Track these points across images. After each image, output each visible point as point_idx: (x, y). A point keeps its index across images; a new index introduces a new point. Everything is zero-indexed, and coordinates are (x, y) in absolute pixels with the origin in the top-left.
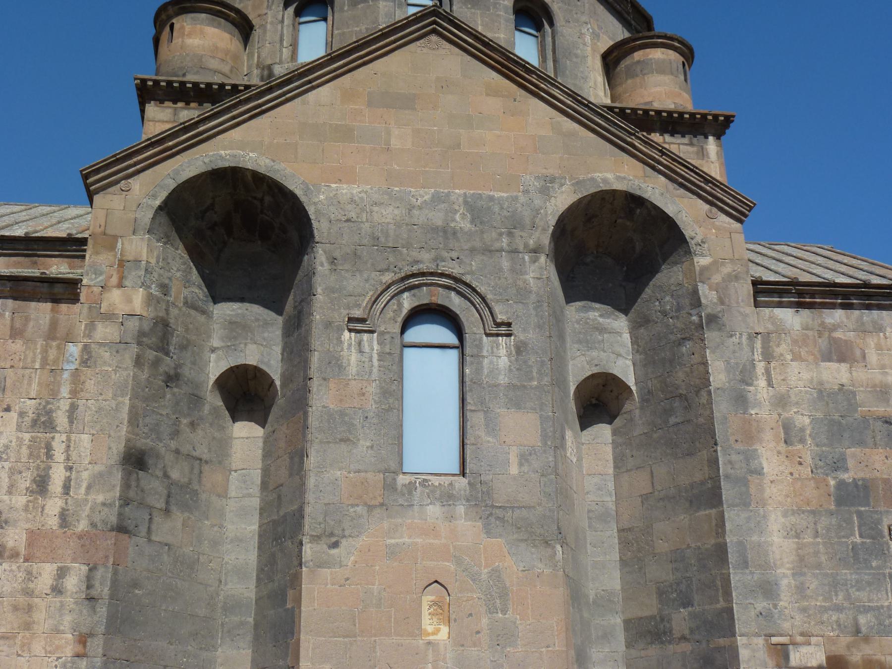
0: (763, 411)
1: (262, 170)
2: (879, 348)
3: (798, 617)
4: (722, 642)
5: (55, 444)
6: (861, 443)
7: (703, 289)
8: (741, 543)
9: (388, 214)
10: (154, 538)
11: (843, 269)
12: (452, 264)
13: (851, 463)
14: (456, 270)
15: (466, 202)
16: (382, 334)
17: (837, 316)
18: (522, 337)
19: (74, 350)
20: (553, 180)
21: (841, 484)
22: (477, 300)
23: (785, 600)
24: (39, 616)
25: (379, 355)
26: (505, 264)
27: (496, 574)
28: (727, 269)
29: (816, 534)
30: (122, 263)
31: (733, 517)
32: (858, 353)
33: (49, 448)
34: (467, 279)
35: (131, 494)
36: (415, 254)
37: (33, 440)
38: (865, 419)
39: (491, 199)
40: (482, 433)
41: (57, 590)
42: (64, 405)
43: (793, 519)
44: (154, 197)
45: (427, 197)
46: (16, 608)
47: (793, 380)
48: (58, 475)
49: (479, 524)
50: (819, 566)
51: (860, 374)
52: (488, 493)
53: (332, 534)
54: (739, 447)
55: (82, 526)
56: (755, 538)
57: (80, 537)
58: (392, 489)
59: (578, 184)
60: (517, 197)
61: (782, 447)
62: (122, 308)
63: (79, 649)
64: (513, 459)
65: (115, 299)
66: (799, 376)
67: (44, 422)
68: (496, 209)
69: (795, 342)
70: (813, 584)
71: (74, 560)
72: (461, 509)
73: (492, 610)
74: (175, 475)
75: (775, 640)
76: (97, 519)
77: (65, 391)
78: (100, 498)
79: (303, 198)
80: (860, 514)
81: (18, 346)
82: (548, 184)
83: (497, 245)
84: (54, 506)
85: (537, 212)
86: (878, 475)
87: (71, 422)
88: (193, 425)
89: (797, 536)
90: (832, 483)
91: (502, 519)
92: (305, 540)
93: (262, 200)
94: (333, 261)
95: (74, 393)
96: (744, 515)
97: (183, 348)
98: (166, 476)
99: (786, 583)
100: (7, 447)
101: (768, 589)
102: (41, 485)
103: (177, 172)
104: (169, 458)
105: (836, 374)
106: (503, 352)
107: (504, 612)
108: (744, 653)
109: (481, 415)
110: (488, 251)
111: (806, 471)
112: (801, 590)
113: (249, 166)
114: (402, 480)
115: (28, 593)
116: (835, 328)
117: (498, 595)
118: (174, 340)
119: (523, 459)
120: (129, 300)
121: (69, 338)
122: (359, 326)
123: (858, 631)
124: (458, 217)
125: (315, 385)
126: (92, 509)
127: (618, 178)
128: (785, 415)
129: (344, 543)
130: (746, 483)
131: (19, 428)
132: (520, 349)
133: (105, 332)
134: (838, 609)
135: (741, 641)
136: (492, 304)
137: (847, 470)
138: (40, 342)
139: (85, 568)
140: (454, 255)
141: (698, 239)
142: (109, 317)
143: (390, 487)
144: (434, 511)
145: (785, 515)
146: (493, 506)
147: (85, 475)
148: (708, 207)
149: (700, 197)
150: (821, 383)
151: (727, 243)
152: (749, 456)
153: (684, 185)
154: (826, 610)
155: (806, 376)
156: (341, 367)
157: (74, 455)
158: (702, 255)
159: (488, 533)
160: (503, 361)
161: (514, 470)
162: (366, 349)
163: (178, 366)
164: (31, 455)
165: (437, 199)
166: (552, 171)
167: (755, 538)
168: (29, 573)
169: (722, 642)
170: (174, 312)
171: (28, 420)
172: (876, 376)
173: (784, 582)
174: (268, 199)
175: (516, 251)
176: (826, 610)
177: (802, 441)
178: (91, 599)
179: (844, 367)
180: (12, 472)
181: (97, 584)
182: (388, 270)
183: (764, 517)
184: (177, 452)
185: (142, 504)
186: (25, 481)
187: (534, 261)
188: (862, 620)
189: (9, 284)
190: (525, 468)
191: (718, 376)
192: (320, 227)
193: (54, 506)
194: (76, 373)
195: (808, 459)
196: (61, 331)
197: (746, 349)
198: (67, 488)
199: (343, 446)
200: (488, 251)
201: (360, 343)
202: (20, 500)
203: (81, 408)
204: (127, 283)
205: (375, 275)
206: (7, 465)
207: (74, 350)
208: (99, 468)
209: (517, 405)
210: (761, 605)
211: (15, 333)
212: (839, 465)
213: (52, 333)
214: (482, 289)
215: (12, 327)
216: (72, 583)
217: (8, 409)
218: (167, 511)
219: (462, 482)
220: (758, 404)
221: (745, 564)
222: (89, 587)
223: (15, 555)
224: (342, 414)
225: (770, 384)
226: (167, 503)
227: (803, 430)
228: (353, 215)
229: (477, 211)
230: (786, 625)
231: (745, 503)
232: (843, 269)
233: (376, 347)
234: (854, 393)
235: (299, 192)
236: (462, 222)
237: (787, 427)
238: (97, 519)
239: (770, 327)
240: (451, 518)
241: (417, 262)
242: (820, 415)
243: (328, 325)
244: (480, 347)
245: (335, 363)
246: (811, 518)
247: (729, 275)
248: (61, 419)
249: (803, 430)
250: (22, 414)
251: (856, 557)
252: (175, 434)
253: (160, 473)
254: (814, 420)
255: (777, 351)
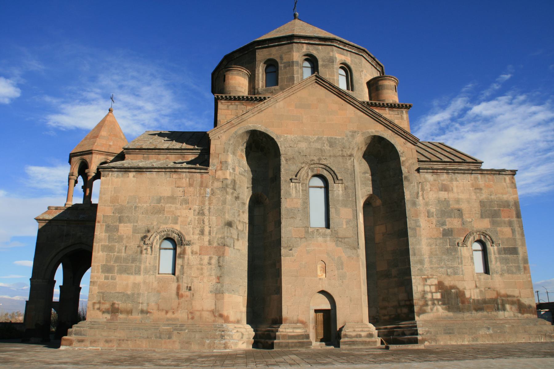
0: (421, 208)
1: (263, 130)
2: (457, 187)
3: (430, 270)
4: (407, 278)
5: (205, 220)
6: (451, 217)
7: (403, 168)
8: (413, 248)
9: (303, 146)
10: (235, 248)
11: (447, 154)
12: (325, 161)
13: (447, 223)
14: (325, 162)
15: (328, 140)
16: (302, 184)
17: (445, 176)
18: (346, 184)
19: (208, 190)
20: (355, 132)
21: (444, 230)
22: (332, 172)
23: (427, 265)
24: (205, 271)
25: (302, 190)
26: (341, 159)
27: (340, 258)
28: (410, 162)
29: (436, 245)
30: (221, 162)
31: (411, 240)
32: (451, 188)
33: (203, 221)
34: (329, 165)
35: (229, 235)
36: (312, 158)
37: (198, 218)
38: (452, 210)
39: (336, 139)
40: (334, 215)
41: (210, 264)
42: (207, 207)
43: (429, 240)
44: (230, 140)
45: (315, 139)
46: (198, 269)
47: (430, 196)
48: (207, 229)
49: (334, 243)
50: (437, 255)
51: (451, 195)
52: (337, 233)
53: (290, 246)
54: (414, 218)
55: (215, 244)
56: (418, 247)
57: (215, 248)
58: (308, 233)
59: (363, 134)
60: (344, 138)
61: (427, 218)
62: (222, 177)
63: (218, 281)
64: (344, 223)
65: (219, 173)
66: (432, 196)
67: (201, 213)
68: (337, 142)
69: (431, 185)
70: (434, 260)
71: (214, 255)
72: (328, 239)
73: (338, 269)
74: (239, 228)
75: (423, 277)
76: (220, 242)
77: (207, 203)
78: (220, 236)
79: (276, 140)
80: (449, 239)
81: (191, 189)
82: (353, 134)
83: (338, 154)
84: (206, 238)
85: (350, 143)
86: (455, 227)
87: (209, 213)
88: (243, 212)
89: (430, 246)
90: (441, 229)
91: (341, 242)
92: (282, 248)
93: (262, 140)
94: (286, 160)
95: (210, 204)
96: (415, 240)
97: (239, 188)
98: (237, 228)
99: (427, 260)
100: (191, 221)
101: (421, 262)
102: (202, 232)
103: (236, 132)
104: (238, 223)
105: (443, 195)
106: (340, 189)
107: (342, 269)
108: (413, 281)
109: (334, 209)
110: (335, 156)
111: (434, 226)
112: (431, 262)
113: (259, 129)
114: (310, 230)
115: (202, 265)
116: (444, 180)
117: (340, 265)
118: (237, 186)
119: (347, 223)
120: (224, 174)
121: (207, 187)
122: (295, 181)
123: (447, 274)
124: (325, 145)
125: (283, 200)
126: (218, 239)
127: (376, 131)
128: (428, 208)
129: (294, 249)
130: (415, 230)
131: (194, 215)
132: (346, 188)
133: (217, 184)
134: (442, 267)
135: (413, 277)
136: (337, 174)
137: (446, 225)
138: (198, 188)
139: (217, 257)
140: (324, 157)
141: (402, 151)
142: (218, 180)
143: (307, 232)
144: (320, 239)
145: (427, 239)
146: (338, 238)
147: (215, 229)
148: (404, 141)
149: (402, 137)
150: (439, 198)
151: (411, 153)
152: (416, 221)
153: (397, 133)
154: (438, 268)
155: (435, 196)
156: (290, 195)
157: (211, 223)
158: (403, 157)
159: (337, 246)
160: (341, 192)
161: (345, 227)
162: (298, 189)
163: (239, 194)
164: (198, 223)
165: (318, 139)
166: (355, 129)
167: (418, 247)
168: (201, 259)
169: (407, 278)
170: (237, 176)
171: (196, 212)
172: (456, 196)
173: (426, 260)
174: (264, 139)
175: (344, 156)
176: (438, 268)
177: (433, 216)
178: (220, 266)
179: (446, 193)
180: (193, 228)
181: (221, 262)
182: (304, 163)
183: (421, 240)
184: (240, 221)
185: (231, 237)
186: (197, 231)
187: (350, 159)
188: (449, 271)
189: (187, 170)
190: (348, 226)
191: (407, 196)
192: (282, 149)
193: (206, 238)
194: (210, 198)
195: (434, 222)
196: (204, 185)
197: (416, 187)
198: (210, 233)
199: (292, 220)
200: (335, 156)
201: (296, 187)
202: (196, 237)
203: (212, 208)
204: (223, 168)
205: (300, 165)
206: (191, 226)
207: (208, 190)
208: (219, 227)
209: (346, 206)
210: (419, 266)
211: (191, 185)
212: (443, 224)
213: (201, 185)
214: (333, 169)
215: (189, 184)
216: (214, 261)
217: (190, 209)
218: (238, 240)
219: (328, 231)
220: (420, 205)
221: (415, 254)
222: (219, 263)
223: (196, 253)
224: (292, 210)
225: (424, 199)
226: (238, 237)
227: (433, 213)
228: (292, 145)
229: (332, 143)
230: (426, 272)
231: (415, 236)
232: (447, 154)
233: (301, 188)
234: (449, 201)
235: (275, 138)
236: (327, 147)
237: (428, 212)
238: (220, 242)
239: (424, 180)
240: (326, 241)
241: (313, 160)
242: (438, 208)
243: (286, 181)
244: (333, 187)
245: (289, 194)
246: (435, 240)
247: (411, 163)
248: (206, 212)
249: (433, 213)
250: (194, 210)
251: (447, 252)
252: (239, 215)
253: (235, 228)
254: (436, 210)
255: (426, 188)
